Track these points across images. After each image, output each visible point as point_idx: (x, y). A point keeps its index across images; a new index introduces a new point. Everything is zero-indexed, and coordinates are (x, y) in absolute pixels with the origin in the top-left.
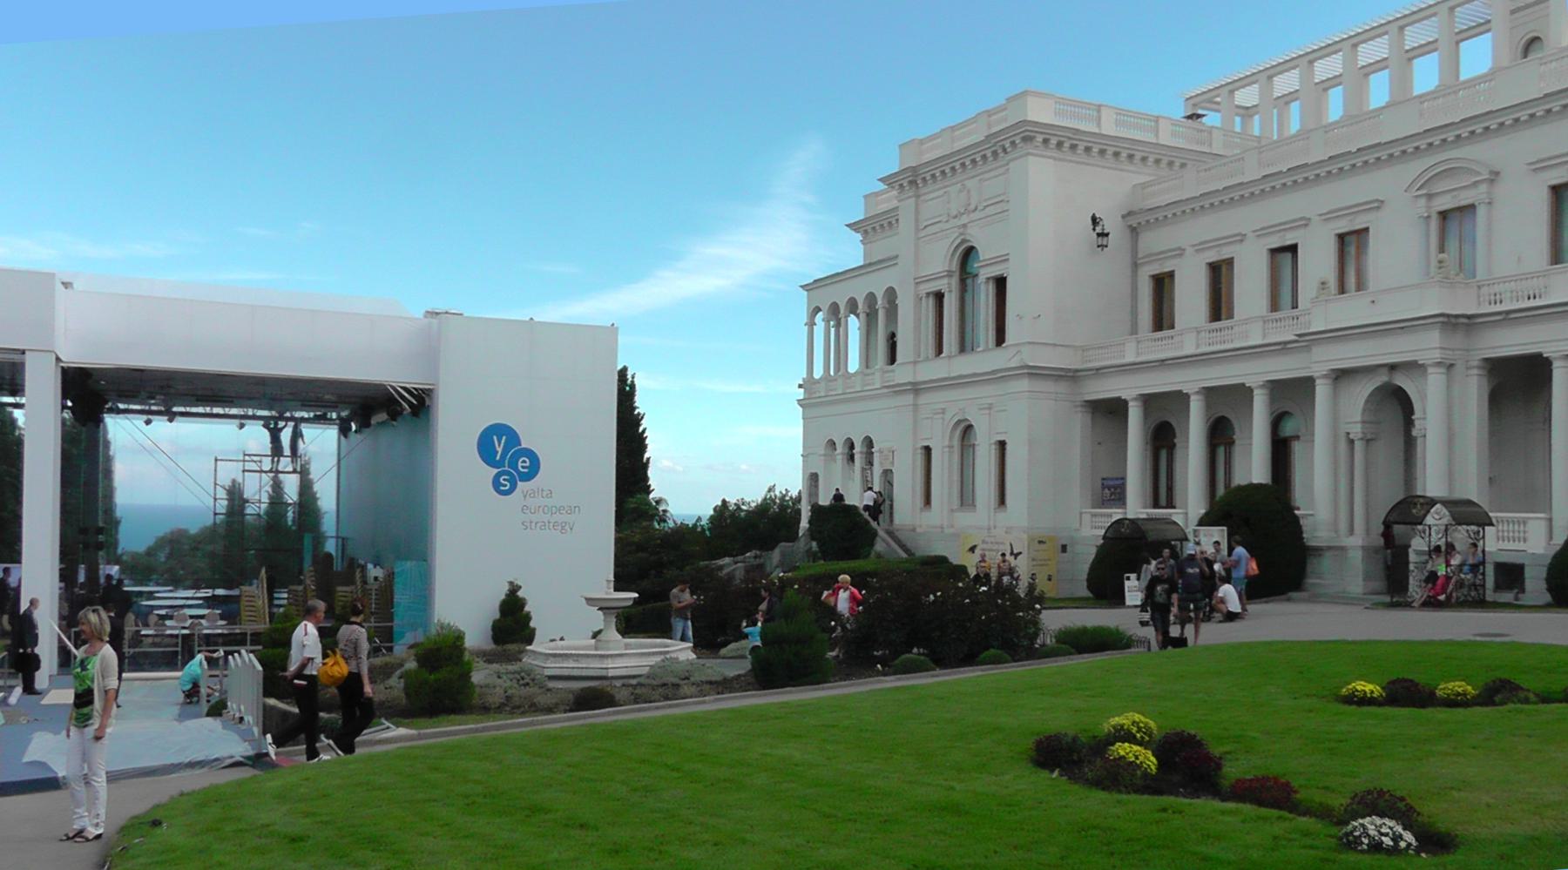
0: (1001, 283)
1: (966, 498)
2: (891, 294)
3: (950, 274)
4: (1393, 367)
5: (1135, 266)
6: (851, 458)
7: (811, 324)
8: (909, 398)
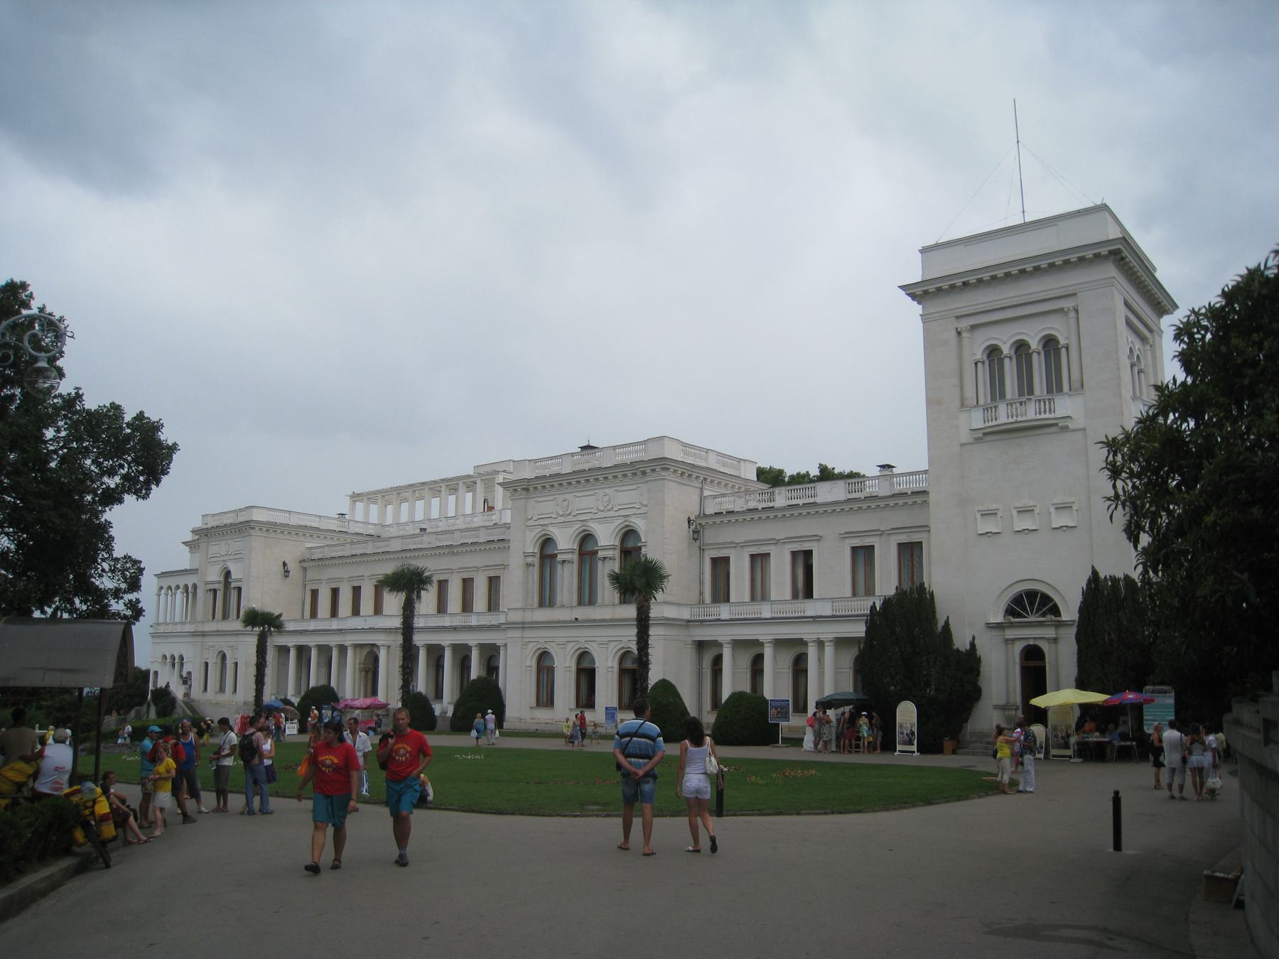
0: (239, 589)
1: (222, 689)
2: (195, 586)
3: (219, 582)
6: (174, 665)
7: (159, 595)
8: (200, 639)
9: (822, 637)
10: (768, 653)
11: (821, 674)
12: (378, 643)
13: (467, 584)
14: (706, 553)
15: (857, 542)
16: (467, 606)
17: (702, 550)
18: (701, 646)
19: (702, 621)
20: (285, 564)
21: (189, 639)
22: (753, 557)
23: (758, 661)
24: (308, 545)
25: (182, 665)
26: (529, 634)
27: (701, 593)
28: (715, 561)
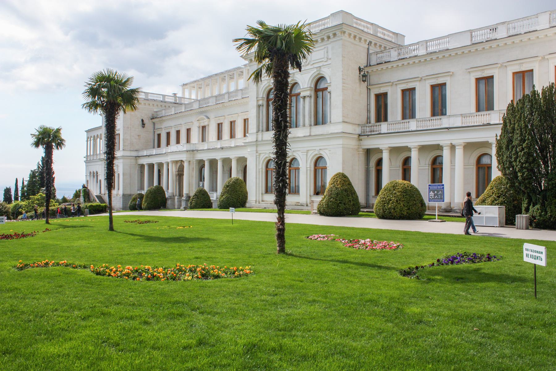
2: (101, 135)
4: (182, 161)
5: (154, 132)
9: (454, 142)
10: (414, 155)
11: (453, 169)
12: (184, 159)
13: (232, 124)
14: (372, 91)
15: (480, 75)
16: (232, 136)
17: (369, 90)
18: (368, 152)
19: (368, 135)
20: (142, 121)
21: (100, 163)
22: (403, 91)
23: (407, 161)
24: (155, 110)
25: (97, 176)
26: (260, 149)
27: (368, 118)
28: (378, 96)
